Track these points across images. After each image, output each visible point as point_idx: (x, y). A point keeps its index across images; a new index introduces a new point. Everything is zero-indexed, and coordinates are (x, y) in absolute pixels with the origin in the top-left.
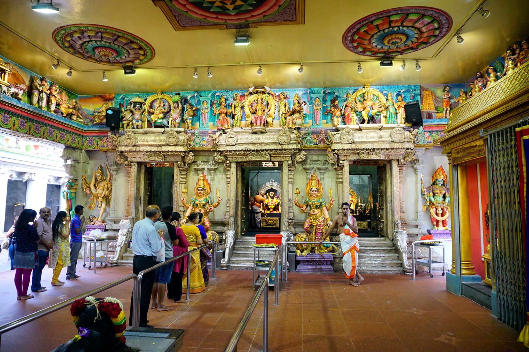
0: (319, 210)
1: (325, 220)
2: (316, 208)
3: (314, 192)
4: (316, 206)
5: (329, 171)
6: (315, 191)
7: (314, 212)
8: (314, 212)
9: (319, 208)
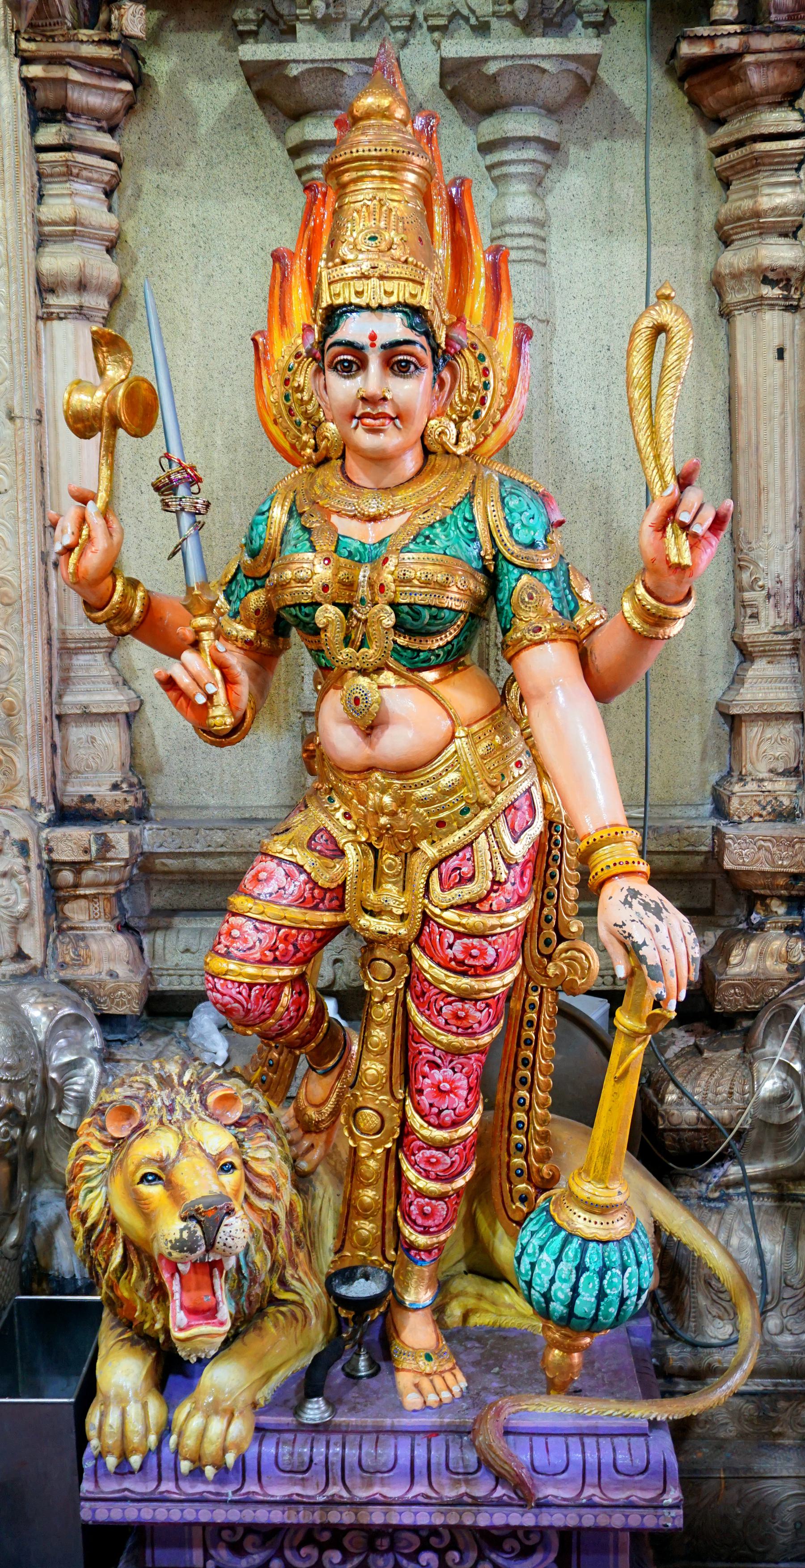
0: (465, 696)
1: (558, 868)
2: (413, 664)
3: (373, 378)
4: (412, 621)
5: (618, 123)
6: (397, 361)
7: (371, 727)
8: (371, 727)
9: (452, 661)
